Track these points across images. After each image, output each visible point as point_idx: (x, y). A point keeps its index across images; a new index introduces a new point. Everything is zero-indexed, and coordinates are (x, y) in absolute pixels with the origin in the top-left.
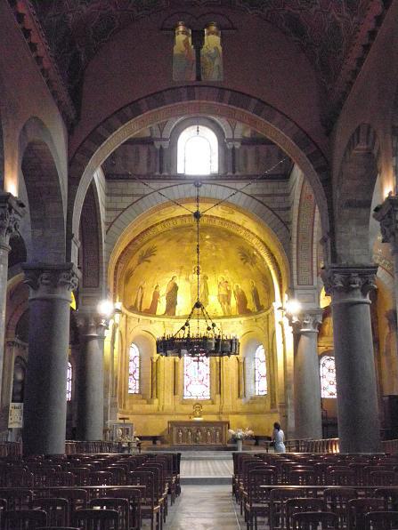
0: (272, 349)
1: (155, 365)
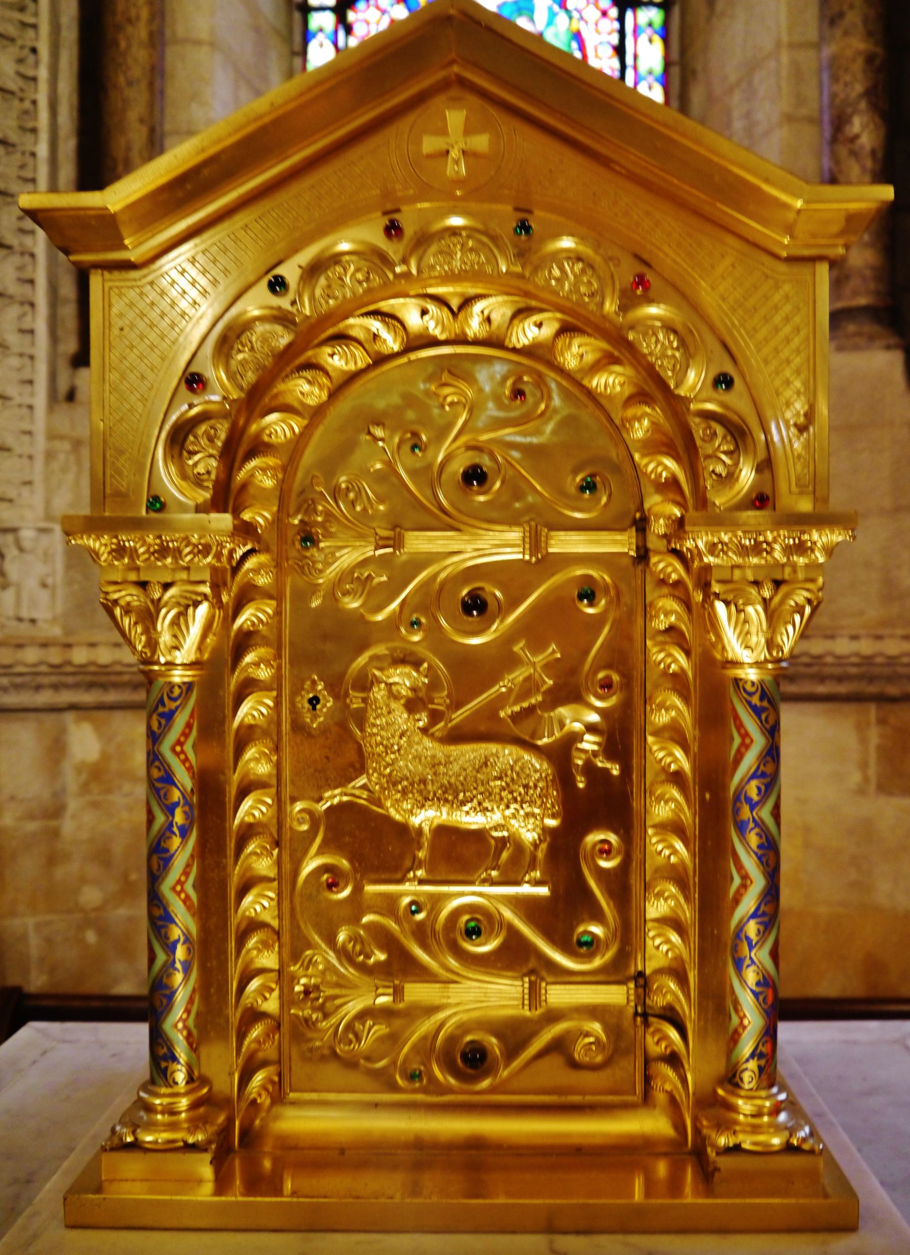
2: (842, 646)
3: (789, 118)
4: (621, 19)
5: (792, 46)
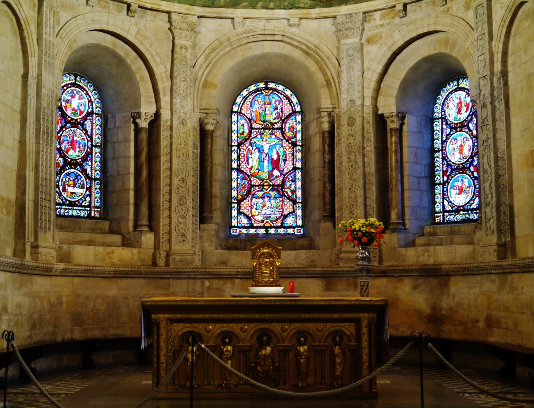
0: (504, 74)
1: (144, 136)
2: (318, 269)
3: (319, 180)
4: (293, 149)
5: (319, 167)
